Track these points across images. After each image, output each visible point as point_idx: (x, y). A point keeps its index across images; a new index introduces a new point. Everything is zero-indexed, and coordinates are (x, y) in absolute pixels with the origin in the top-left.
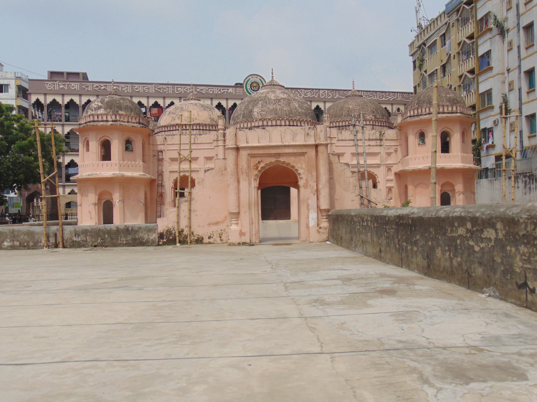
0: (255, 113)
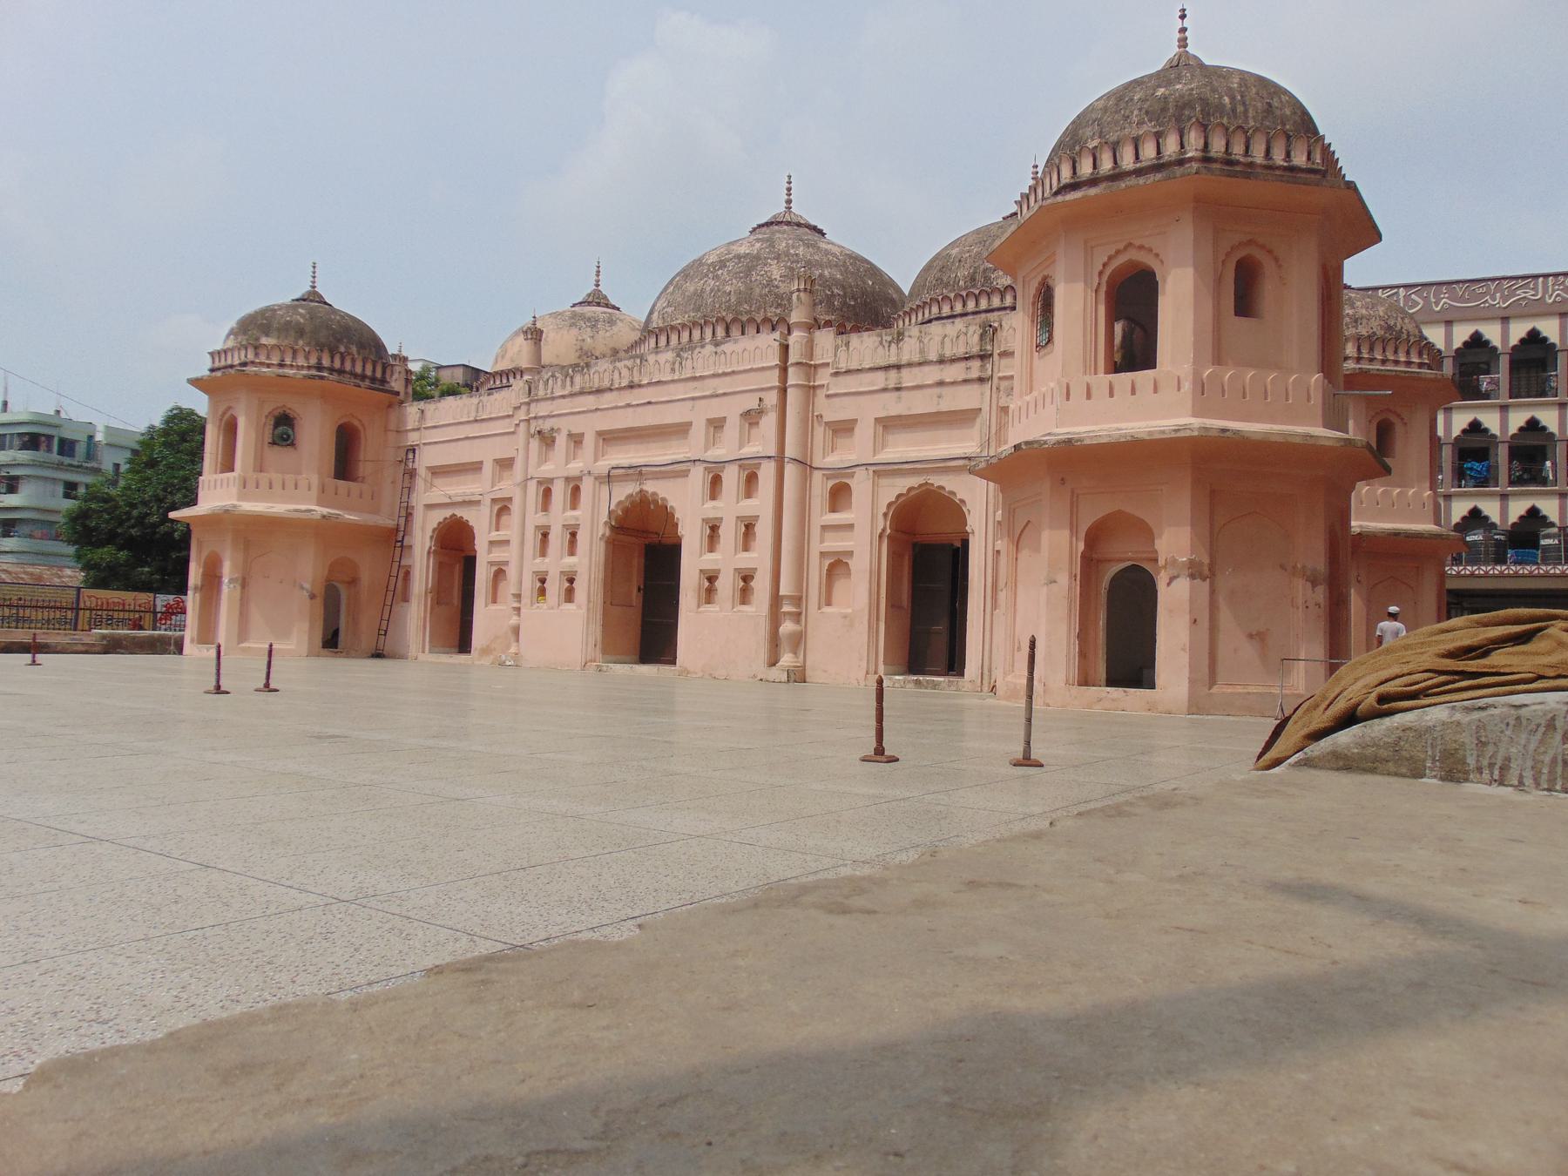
0: (655, 315)
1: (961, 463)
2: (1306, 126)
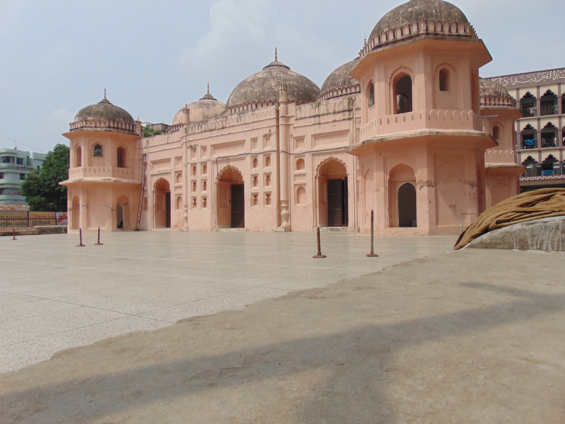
0: (230, 102)
1: (343, 149)
2: (463, 19)
